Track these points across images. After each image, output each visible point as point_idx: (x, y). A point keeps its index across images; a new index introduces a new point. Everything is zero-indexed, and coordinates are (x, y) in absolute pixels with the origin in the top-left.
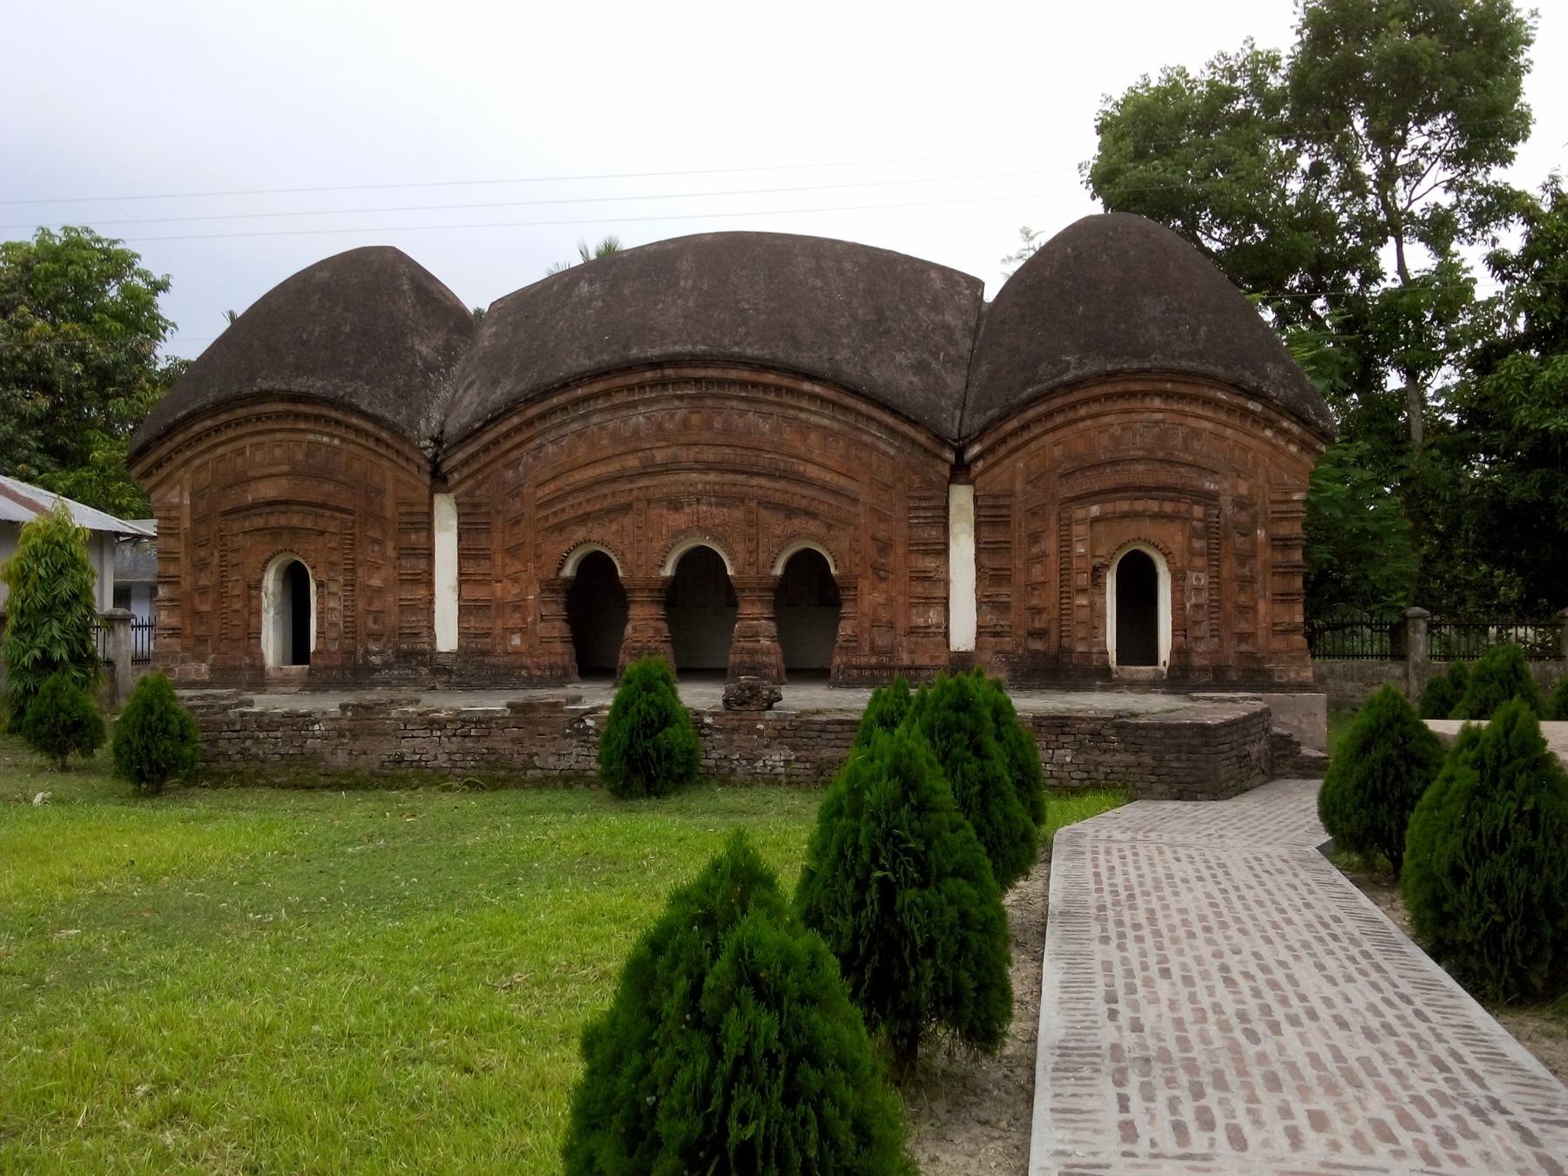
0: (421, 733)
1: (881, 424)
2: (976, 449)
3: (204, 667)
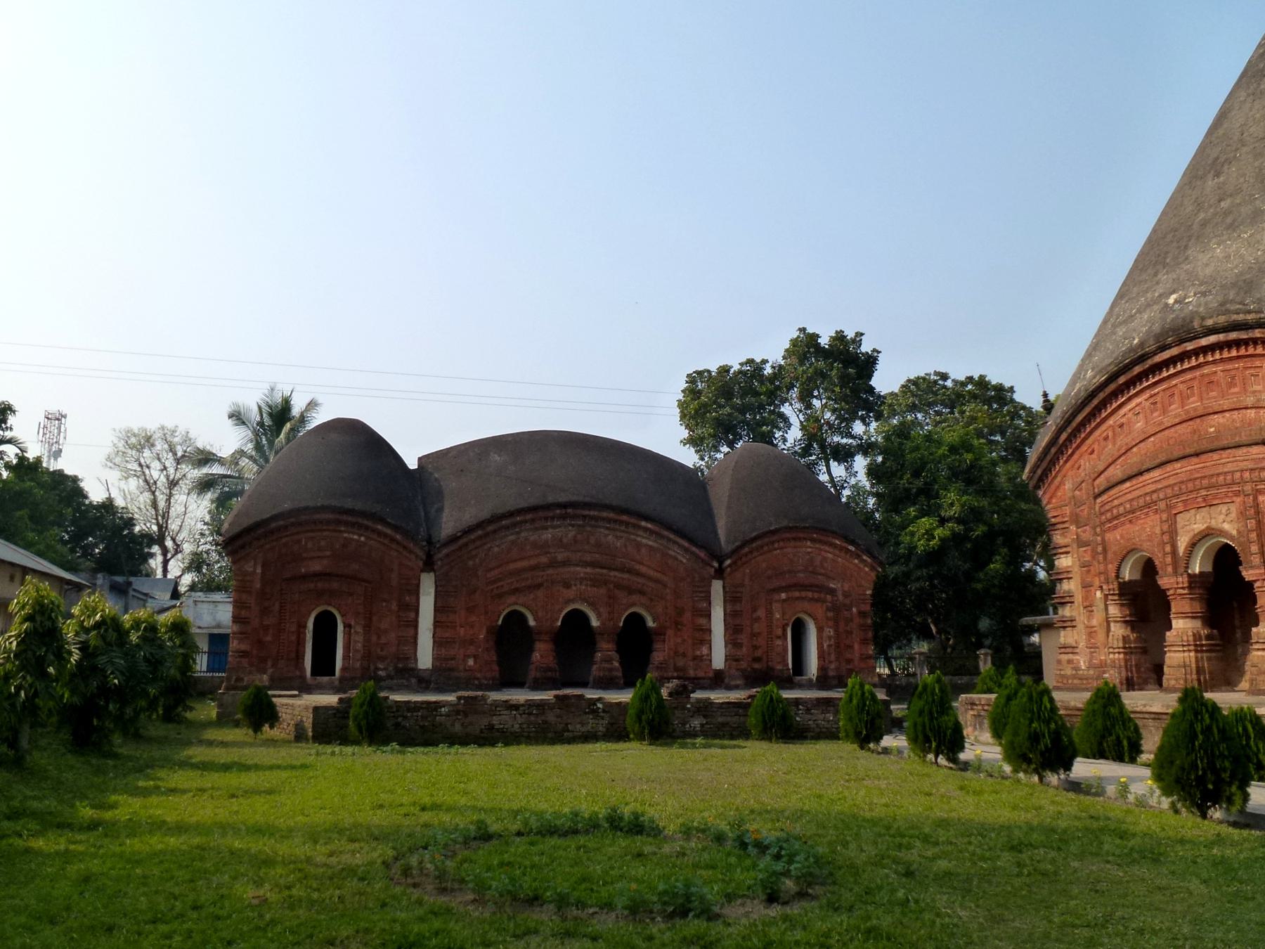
0: (505, 712)
1: (680, 546)
2: (728, 562)
3: (265, 677)
